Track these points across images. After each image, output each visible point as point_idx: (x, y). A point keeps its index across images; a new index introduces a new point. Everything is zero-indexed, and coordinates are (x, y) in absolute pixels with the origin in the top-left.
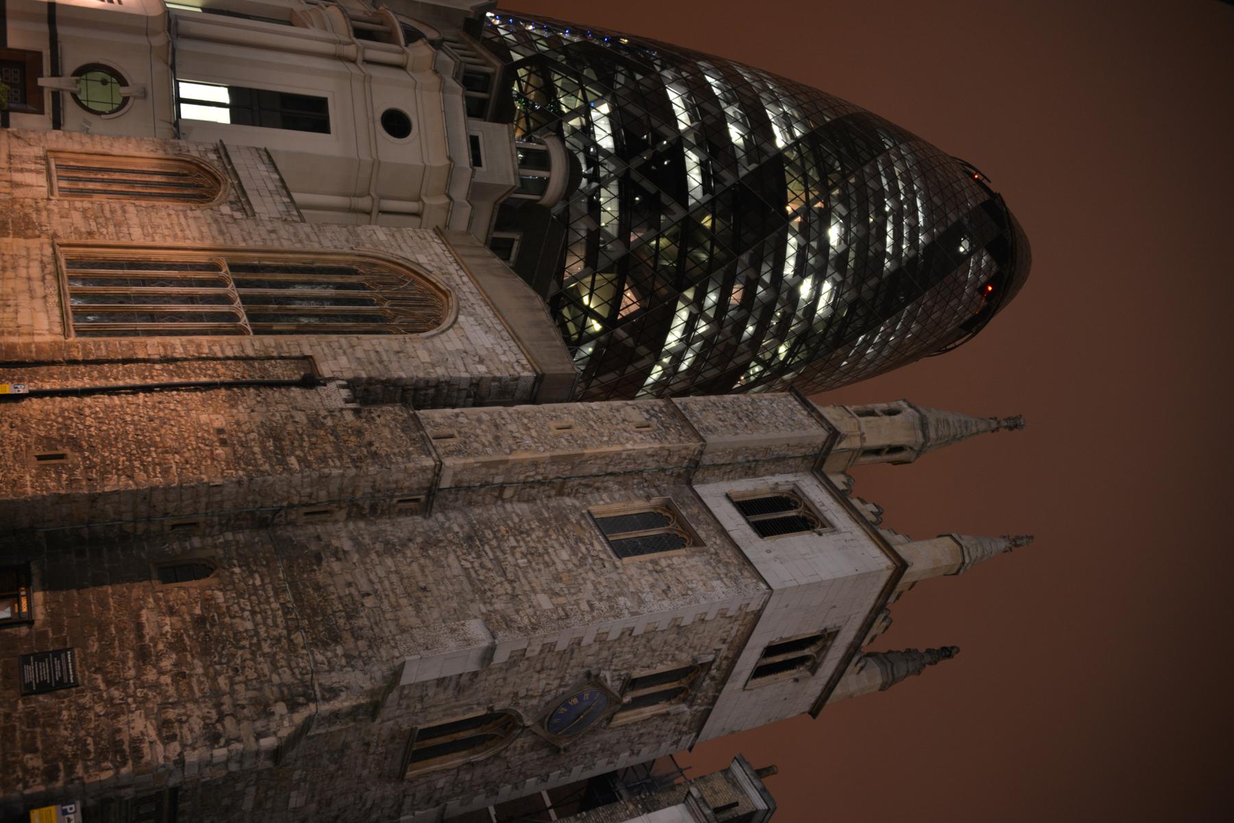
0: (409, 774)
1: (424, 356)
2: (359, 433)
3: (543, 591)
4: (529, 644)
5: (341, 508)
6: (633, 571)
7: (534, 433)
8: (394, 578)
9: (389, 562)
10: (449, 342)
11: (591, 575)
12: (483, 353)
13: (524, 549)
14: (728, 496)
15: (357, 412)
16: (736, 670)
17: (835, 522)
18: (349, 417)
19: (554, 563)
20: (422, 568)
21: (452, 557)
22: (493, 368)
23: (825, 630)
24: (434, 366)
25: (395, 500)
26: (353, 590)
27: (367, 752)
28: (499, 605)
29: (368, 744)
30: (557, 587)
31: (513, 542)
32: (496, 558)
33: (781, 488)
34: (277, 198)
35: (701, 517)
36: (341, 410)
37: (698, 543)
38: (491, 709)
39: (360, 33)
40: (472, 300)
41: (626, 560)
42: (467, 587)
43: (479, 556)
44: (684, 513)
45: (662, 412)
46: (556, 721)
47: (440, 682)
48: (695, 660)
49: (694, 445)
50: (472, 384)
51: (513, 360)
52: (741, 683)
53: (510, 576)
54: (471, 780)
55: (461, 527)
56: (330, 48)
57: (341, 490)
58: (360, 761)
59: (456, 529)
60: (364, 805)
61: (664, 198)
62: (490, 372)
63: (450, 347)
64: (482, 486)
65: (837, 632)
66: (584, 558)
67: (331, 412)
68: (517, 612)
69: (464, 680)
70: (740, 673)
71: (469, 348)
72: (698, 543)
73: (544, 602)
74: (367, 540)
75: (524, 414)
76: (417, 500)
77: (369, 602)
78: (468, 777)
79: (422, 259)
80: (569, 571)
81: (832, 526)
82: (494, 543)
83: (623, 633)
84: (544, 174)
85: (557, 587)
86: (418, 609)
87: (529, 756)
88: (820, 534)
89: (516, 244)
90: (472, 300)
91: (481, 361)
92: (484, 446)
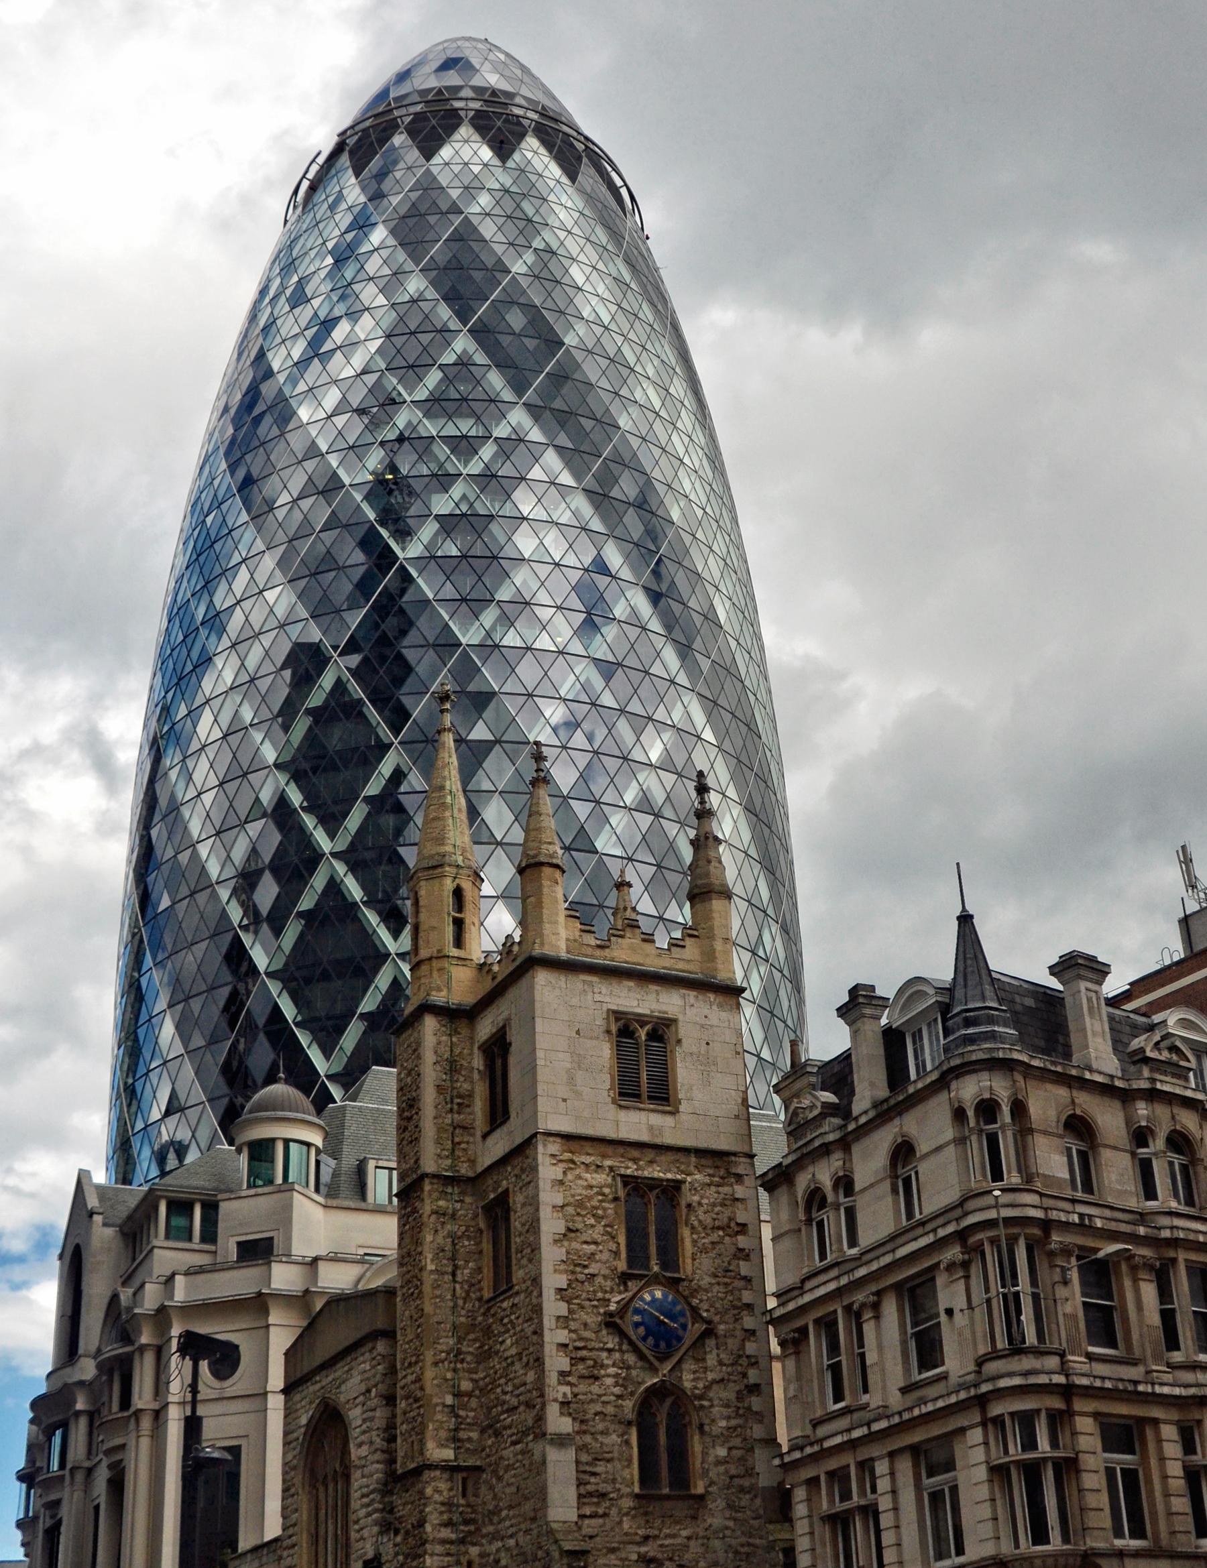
0: (700, 1490)
1: (364, 1451)
2: (407, 1533)
3: (526, 1374)
4: (555, 1400)
5: (467, 1552)
6: (521, 1273)
7: (414, 1359)
8: (511, 1513)
9: (504, 1513)
10: (355, 1415)
11: (520, 1321)
12: (363, 1388)
13: (503, 1381)
14: (485, 1136)
15: (397, 1532)
16: (645, 1137)
17: (505, 1015)
18: (399, 1539)
19: (512, 1356)
20: (509, 1485)
21: (505, 1453)
22: (372, 1383)
23: (608, 1032)
24: (371, 1443)
25: (462, 1502)
26: (515, 1553)
27: (656, 1537)
28: (530, 1422)
29: (646, 1538)
30: (525, 1359)
31: (499, 1390)
32: (508, 1411)
33: (481, 1068)
34: (264, 1559)
35: (495, 1178)
36: (395, 1545)
37: (506, 1192)
38: (629, 1423)
39: (126, 1402)
40: (330, 1378)
41: (515, 1281)
42: (519, 1447)
43: (505, 1428)
44: (492, 1196)
45: (405, 1208)
46: (663, 1344)
47: (580, 1484)
48: (616, 1199)
49: (427, 1187)
50: (387, 1404)
51: (367, 1354)
52: (669, 1121)
53: (514, 1402)
54: (728, 1418)
55: (490, 1437)
56: (145, 1442)
57: (448, 1554)
58: (667, 1542)
59: (490, 1442)
60: (727, 1528)
61: (373, 788)
62: (376, 1386)
63: (359, 1422)
64: (457, 1416)
65: (615, 1012)
66: (511, 1321)
67: (397, 1554)
68: (534, 1406)
69: (584, 1458)
70: (651, 1128)
71: (361, 1398)
72: (506, 1192)
73: (531, 1377)
74: (491, 1529)
75: (403, 1364)
76: (464, 1480)
77: (521, 1540)
78: (723, 1423)
79: (304, 1420)
80: (517, 1342)
81: (504, 1027)
82: (499, 1408)
83: (562, 1299)
84: (280, 1148)
85: (525, 1359)
86: (527, 1499)
87: (711, 1360)
88: (510, 1044)
89: (381, 1164)
90: (330, 1378)
91: (368, 1391)
92: (419, 1414)
